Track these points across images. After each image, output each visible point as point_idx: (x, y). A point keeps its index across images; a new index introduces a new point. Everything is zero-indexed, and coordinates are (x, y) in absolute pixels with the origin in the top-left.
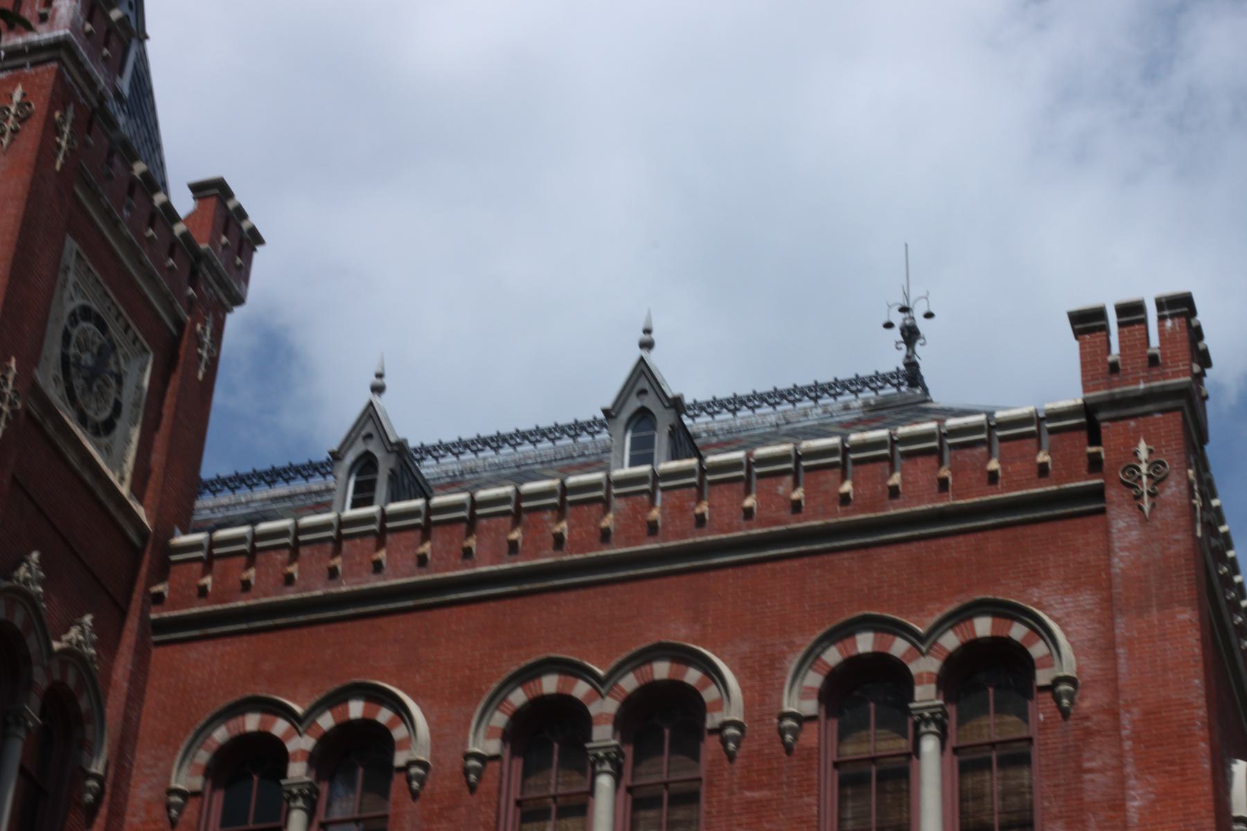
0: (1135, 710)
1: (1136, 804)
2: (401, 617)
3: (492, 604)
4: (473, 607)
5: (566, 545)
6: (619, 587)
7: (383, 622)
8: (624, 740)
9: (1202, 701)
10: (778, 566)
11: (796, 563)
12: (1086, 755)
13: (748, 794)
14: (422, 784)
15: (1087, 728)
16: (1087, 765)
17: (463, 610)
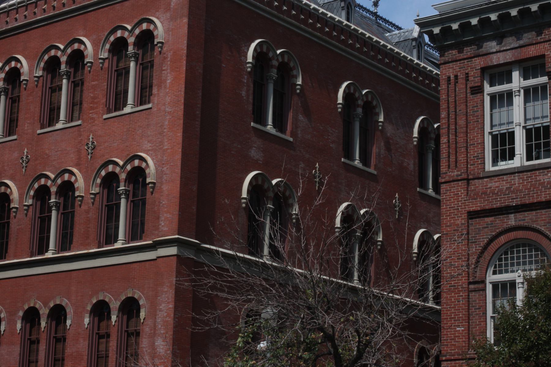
0: (171, 52)
1: (169, 81)
2: (23, 34)
3: (42, 28)
4: (38, 29)
5: (56, 9)
6: (69, 20)
7: (19, 36)
8: (70, 68)
9: (186, 48)
10: (103, 10)
11: (106, 9)
12: (164, 65)
13: (93, 83)
14: (26, 86)
15: (164, 57)
16: (164, 68)
17: (36, 30)
